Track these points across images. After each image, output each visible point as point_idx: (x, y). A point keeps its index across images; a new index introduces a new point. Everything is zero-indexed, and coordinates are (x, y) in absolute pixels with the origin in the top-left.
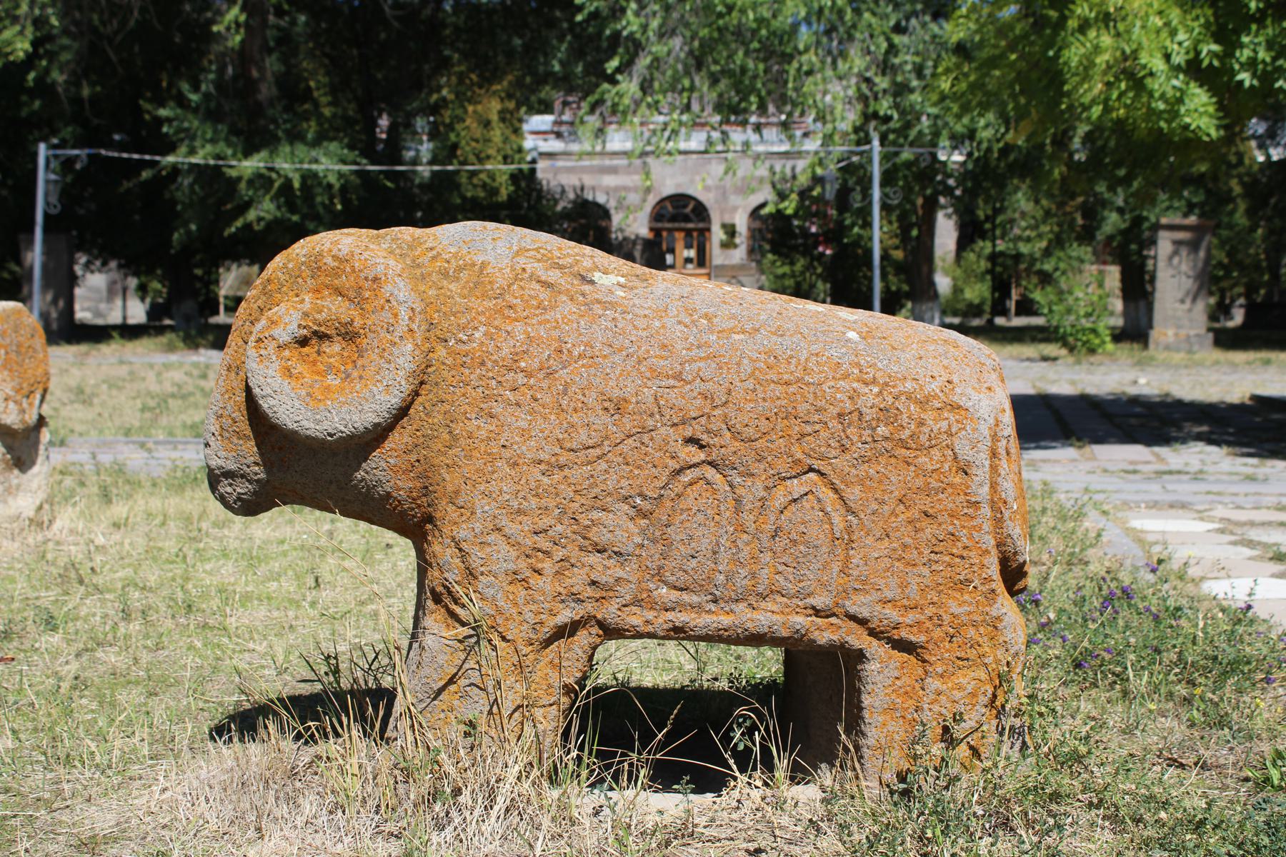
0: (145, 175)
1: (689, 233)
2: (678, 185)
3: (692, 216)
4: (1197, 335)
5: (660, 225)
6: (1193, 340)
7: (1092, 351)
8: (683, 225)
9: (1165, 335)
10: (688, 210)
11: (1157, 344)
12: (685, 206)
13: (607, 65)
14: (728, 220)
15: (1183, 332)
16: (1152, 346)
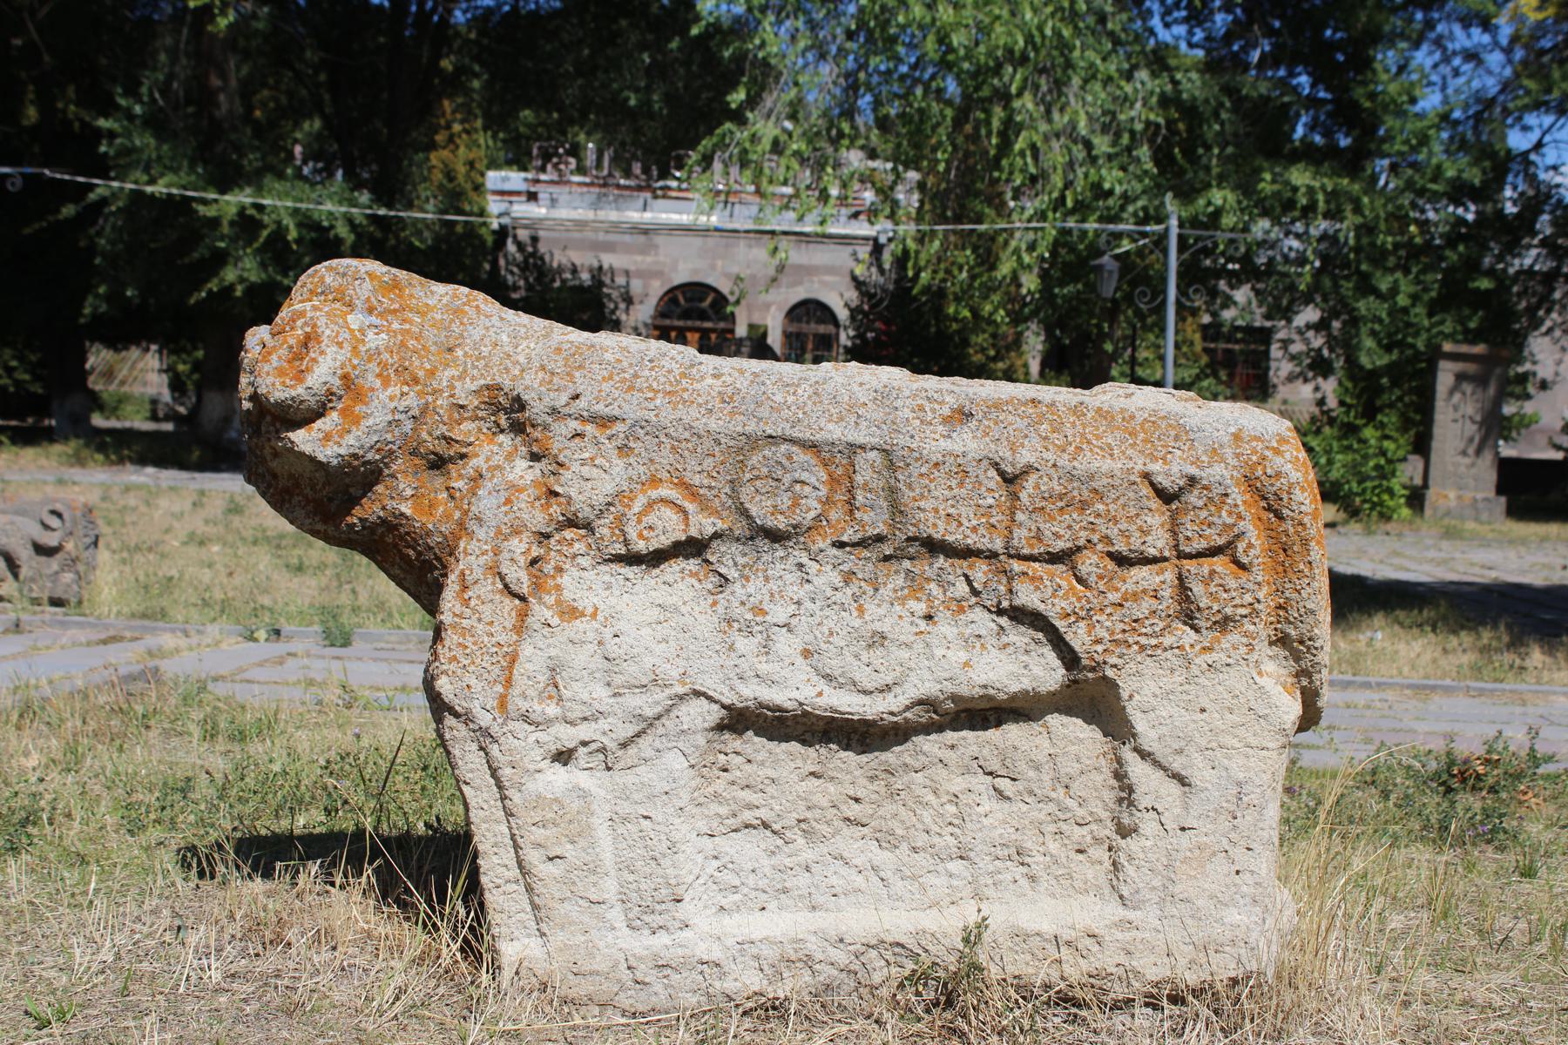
0: (68, 211)
1: (705, 333)
2: (695, 271)
3: (710, 312)
4: (1486, 499)
5: (667, 322)
6: (1480, 505)
7: (1386, 517)
8: (698, 324)
9: (1446, 497)
10: (706, 304)
11: (1435, 509)
12: (702, 300)
13: (729, 98)
14: (756, 319)
15: (1468, 495)
16: (1428, 512)
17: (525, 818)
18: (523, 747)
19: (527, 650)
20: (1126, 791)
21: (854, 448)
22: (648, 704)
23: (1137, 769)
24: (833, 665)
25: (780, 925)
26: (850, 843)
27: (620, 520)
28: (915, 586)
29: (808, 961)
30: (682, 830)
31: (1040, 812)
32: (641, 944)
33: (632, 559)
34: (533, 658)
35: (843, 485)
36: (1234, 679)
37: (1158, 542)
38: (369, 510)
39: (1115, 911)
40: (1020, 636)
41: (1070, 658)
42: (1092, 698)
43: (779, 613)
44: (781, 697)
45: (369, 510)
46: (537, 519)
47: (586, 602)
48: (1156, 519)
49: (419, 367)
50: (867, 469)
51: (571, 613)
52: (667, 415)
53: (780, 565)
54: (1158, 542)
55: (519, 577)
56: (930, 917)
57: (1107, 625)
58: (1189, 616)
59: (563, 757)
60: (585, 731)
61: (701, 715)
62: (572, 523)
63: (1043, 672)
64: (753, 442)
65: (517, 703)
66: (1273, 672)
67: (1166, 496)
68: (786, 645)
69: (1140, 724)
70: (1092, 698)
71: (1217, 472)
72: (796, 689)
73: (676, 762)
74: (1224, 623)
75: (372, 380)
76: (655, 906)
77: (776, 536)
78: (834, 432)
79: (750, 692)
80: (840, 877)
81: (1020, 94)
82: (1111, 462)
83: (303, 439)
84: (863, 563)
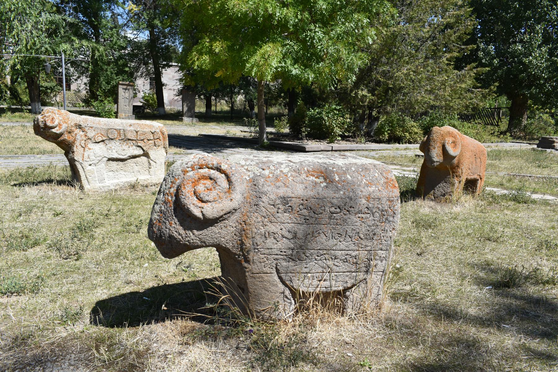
17: (86, 172)
18: (86, 164)
19: (85, 153)
20: (150, 164)
21: (120, 129)
22: (100, 158)
23: (151, 162)
24: (120, 153)
25: (116, 181)
26: (122, 172)
27: (94, 139)
28: (127, 144)
29: (119, 185)
30: (104, 172)
31: (141, 167)
32: (101, 185)
33: (96, 143)
34: (86, 155)
35: (119, 133)
36: (160, 152)
37: (152, 138)
38: (61, 138)
39: (150, 176)
40: (138, 148)
41: (144, 150)
42: (146, 155)
43: (113, 148)
44: (114, 157)
45: (61, 138)
46: (85, 139)
47: (91, 148)
48: (152, 136)
49: (66, 121)
50: (122, 132)
51: (90, 149)
52: (99, 126)
53: (113, 142)
54: (152, 138)
55: (83, 145)
56: (132, 179)
57: (147, 147)
58: (155, 146)
59: (90, 165)
60: (93, 162)
61: (106, 159)
62: (89, 139)
63: (141, 152)
64: (109, 129)
65: (85, 159)
66: (163, 150)
67: (152, 133)
68: (114, 151)
69: (151, 157)
70: (146, 155)
71: (158, 130)
72: (115, 156)
73: (103, 164)
74: (159, 146)
75: (62, 123)
76: (102, 180)
77: (112, 139)
78: (118, 128)
79: (111, 156)
80: (121, 176)
81: (13, 20)
82: (147, 130)
83: (53, 130)
84: (122, 142)
